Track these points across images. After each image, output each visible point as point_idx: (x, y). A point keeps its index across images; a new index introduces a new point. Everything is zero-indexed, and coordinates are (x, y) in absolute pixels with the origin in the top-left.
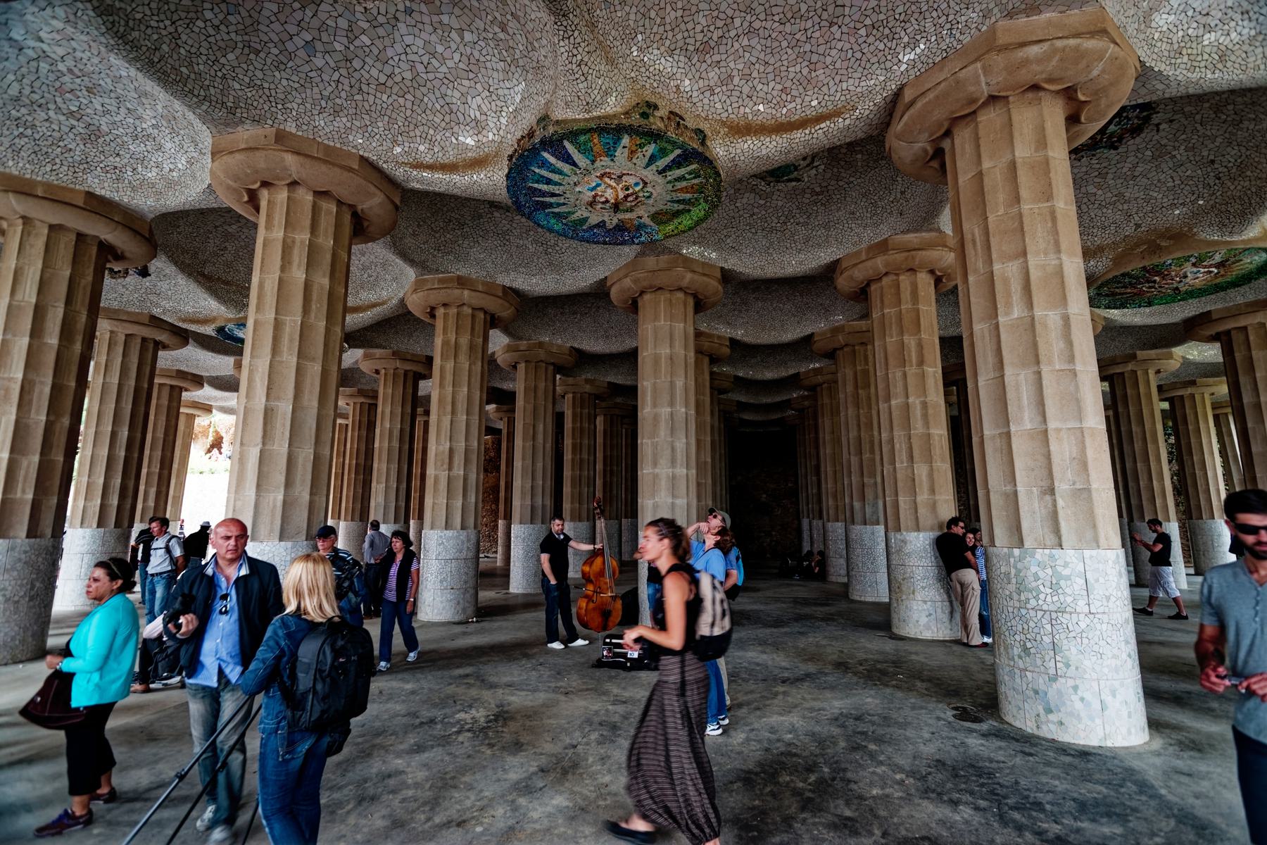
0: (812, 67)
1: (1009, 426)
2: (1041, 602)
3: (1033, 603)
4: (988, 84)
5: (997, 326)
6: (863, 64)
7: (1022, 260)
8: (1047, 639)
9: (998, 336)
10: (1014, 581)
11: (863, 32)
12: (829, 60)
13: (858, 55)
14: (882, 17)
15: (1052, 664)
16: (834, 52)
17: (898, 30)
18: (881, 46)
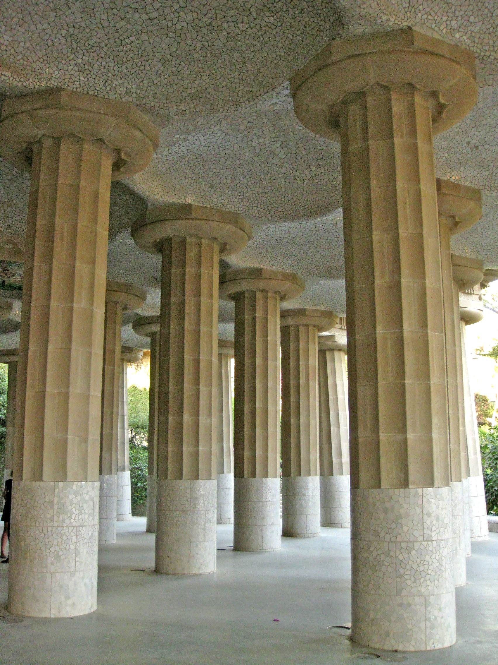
0: (21, 22)
1: (68, 387)
2: (72, 521)
3: (67, 521)
4: (110, 135)
5: (71, 309)
6: (48, 50)
7: (91, 266)
8: (72, 547)
9: (71, 317)
10: (56, 507)
11: (64, 32)
12: (33, 28)
13: (50, 43)
14: (80, 36)
15: (73, 564)
16: (40, 27)
17: (81, 52)
18: (65, 52)
